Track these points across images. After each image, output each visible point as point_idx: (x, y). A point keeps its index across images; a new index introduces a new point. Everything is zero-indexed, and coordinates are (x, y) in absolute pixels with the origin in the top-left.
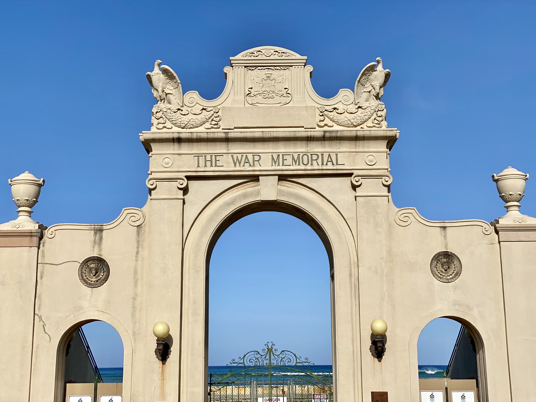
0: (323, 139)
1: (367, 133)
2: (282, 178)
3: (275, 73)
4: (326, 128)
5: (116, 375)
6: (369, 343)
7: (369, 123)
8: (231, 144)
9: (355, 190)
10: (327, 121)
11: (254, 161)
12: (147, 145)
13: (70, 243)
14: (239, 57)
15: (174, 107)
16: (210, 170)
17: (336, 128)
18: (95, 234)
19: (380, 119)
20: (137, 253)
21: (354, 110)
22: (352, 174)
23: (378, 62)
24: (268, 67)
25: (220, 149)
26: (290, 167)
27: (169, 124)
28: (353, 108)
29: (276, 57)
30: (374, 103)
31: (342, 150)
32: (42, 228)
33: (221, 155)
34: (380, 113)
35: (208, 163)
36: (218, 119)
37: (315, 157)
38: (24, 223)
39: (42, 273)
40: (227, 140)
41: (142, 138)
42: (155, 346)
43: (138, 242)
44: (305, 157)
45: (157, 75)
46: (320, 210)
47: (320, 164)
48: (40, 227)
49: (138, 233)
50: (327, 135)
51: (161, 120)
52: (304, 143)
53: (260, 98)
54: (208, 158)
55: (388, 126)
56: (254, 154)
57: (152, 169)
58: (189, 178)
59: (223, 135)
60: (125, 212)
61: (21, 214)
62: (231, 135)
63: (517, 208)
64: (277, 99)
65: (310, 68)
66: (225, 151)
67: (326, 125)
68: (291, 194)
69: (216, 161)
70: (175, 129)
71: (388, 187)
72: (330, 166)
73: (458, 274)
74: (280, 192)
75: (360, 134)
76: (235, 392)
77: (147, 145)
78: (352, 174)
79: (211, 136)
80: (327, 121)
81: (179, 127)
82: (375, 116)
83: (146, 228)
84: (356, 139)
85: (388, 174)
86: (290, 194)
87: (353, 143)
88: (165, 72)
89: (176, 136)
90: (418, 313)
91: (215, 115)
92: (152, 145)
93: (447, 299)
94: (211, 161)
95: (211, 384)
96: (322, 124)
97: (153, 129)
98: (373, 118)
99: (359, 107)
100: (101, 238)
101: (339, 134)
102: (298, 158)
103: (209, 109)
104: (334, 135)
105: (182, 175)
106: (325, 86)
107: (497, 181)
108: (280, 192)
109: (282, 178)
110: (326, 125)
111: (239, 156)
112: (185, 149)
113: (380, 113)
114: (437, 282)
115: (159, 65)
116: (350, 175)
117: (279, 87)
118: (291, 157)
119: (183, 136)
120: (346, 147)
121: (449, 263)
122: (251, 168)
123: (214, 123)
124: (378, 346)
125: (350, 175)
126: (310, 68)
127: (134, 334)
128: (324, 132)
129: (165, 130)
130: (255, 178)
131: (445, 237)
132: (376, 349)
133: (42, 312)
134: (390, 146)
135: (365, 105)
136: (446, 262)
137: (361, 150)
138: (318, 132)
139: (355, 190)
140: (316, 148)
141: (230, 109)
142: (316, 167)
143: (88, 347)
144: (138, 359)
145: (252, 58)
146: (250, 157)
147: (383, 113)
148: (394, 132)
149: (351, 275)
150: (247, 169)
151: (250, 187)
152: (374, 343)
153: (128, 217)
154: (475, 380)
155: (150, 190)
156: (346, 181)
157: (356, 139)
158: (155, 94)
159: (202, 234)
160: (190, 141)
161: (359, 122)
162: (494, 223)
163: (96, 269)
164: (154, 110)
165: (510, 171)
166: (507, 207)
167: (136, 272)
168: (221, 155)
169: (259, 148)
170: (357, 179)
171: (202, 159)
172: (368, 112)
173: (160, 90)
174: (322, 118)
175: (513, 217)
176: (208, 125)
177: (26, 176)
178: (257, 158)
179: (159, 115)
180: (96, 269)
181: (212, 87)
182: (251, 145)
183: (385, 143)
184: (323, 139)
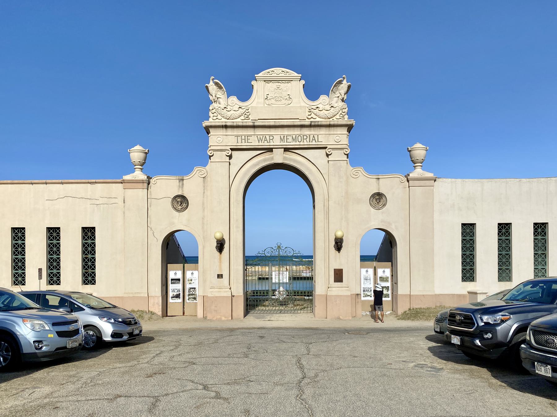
0: (310, 126)
1: (336, 123)
2: (286, 150)
3: (282, 85)
4: (312, 120)
5: (194, 260)
6: (334, 243)
7: (338, 117)
8: (256, 129)
9: (328, 157)
10: (313, 115)
11: (270, 139)
12: (207, 129)
13: (166, 186)
14: (260, 74)
15: (222, 106)
16: (244, 145)
17: (318, 119)
18: (179, 181)
19: (344, 114)
20: (204, 193)
21: (329, 109)
22: (326, 147)
23: (344, 78)
24: (278, 81)
25: (250, 132)
26: (291, 144)
27: (219, 117)
28: (328, 107)
29: (283, 75)
30: (341, 104)
31: (321, 133)
32: (149, 178)
33: (251, 136)
34: (344, 110)
35: (243, 141)
36: (248, 114)
37: (305, 137)
38: (139, 175)
39: (151, 204)
40: (254, 127)
41: (204, 125)
42: (216, 244)
43: (204, 187)
44: (300, 137)
45: (212, 86)
46: (308, 169)
47: (308, 141)
48: (148, 177)
49: (204, 181)
50: (313, 124)
51: (215, 114)
52: (299, 129)
53: (273, 101)
54: (243, 137)
55: (349, 118)
56: (270, 136)
57: (210, 144)
58: (232, 150)
59: (251, 124)
60: (196, 169)
61: (136, 170)
62: (256, 124)
63: (420, 167)
64: (284, 101)
65: (303, 82)
66: (253, 134)
67: (312, 118)
68: (292, 159)
69: (248, 139)
70: (223, 120)
71: (347, 155)
72: (314, 143)
73: (384, 205)
74: (285, 158)
75: (332, 123)
76: (260, 270)
77: (207, 129)
78: (326, 147)
79: (245, 124)
80: (313, 115)
81: (226, 118)
82: (341, 112)
83: (208, 179)
84: (330, 126)
85: (347, 147)
86: (291, 160)
87: (328, 128)
88: (216, 84)
89: (224, 124)
90: (361, 227)
91: (247, 111)
92: (211, 130)
93: (378, 219)
94: (245, 139)
95: (247, 265)
96: (310, 117)
97: (211, 120)
98: (340, 113)
99: (332, 107)
100: (183, 184)
101: (319, 123)
102: (296, 137)
103: (243, 108)
104: (316, 124)
105: (228, 148)
106: (312, 93)
107: (410, 151)
108: (285, 158)
109: (286, 150)
110: (312, 118)
111: (261, 137)
112: (230, 132)
113: (344, 110)
114: (372, 210)
115: (213, 80)
116: (325, 148)
117: (285, 94)
118: (291, 137)
119: (228, 124)
120: (323, 131)
121: (380, 199)
122: (268, 144)
123: (246, 116)
124: (339, 245)
125: (325, 148)
126: (303, 82)
127: (204, 238)
128: (311, 122)
129: (217, 120)
130: (270, 150)
131: (378, 184)
132: (337, 246)
133: (152, 225)
134: (349, 131)
135: (335, 105)
136: (378, 198)
137: (332, 133)
138: (307, 122)
139: (328, 157)
140: (306, 132)
141: (256, 108)
142: (305, 143)
143: (179, 245)
144: (206, 252)
145: (269, 75)
146: (268, 137)
147: (346, 110)
148: (352, 122)
149: (324, 206)
150: (266, 144)
151: (267, 155)
152: (336, 243)
153: (198, 172)
154: (390, 263)
155: (210, 157)
156: (323, 151)
157: (330, 126)
158: (211, 97)
159: (240, 182)
160: (232, 127)
161: (332, 116)
162: (407, 176)
163: (181, 202)
164: (211, 108)
165: (418, 145)
166: (415, 167)
167: (203, 204)
168: (251, 136)
169: (272, 132)
170: (329, 150)
171: (239, 138)
172: (337, 109)
173: (214, 95)
174: (310, 113)
175: (418, 172)
176: (242, 118)
177: (138, 147)
178: (271, 138)
179: (214, 111)
180: (181, 202)
181: (245, 94)
182: (268, 129)
183: (346, 128)
184: (310, 126)
